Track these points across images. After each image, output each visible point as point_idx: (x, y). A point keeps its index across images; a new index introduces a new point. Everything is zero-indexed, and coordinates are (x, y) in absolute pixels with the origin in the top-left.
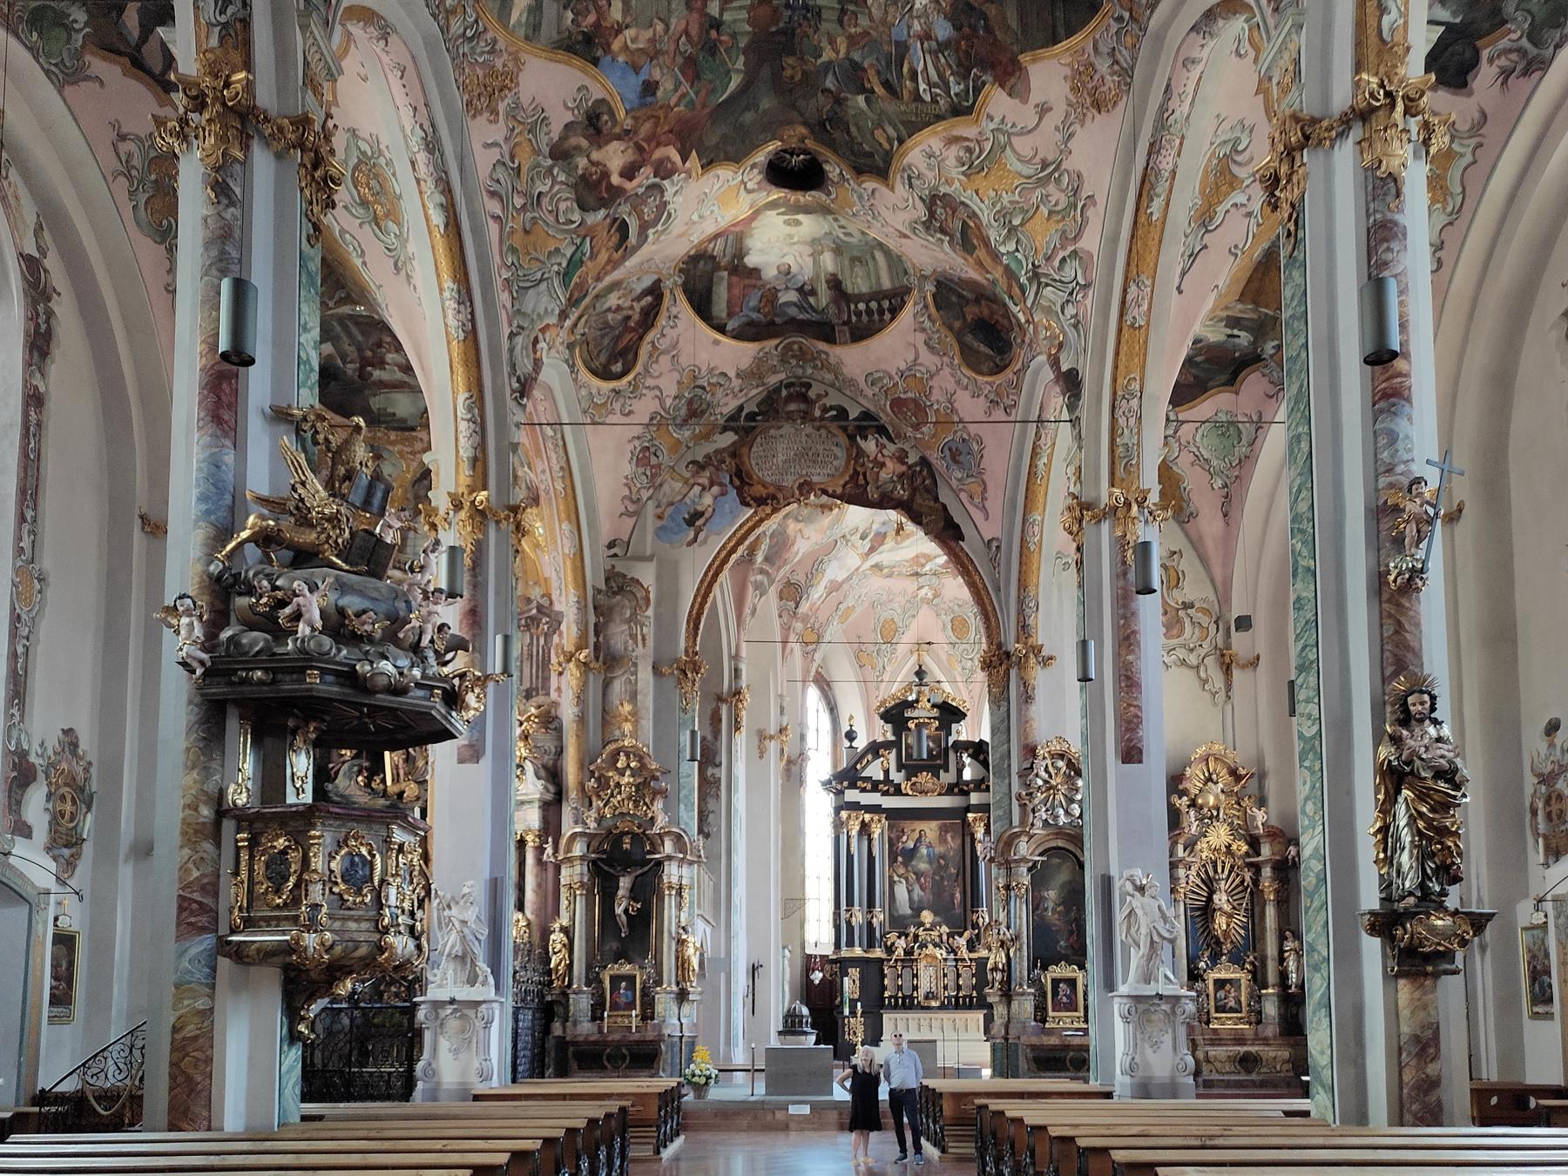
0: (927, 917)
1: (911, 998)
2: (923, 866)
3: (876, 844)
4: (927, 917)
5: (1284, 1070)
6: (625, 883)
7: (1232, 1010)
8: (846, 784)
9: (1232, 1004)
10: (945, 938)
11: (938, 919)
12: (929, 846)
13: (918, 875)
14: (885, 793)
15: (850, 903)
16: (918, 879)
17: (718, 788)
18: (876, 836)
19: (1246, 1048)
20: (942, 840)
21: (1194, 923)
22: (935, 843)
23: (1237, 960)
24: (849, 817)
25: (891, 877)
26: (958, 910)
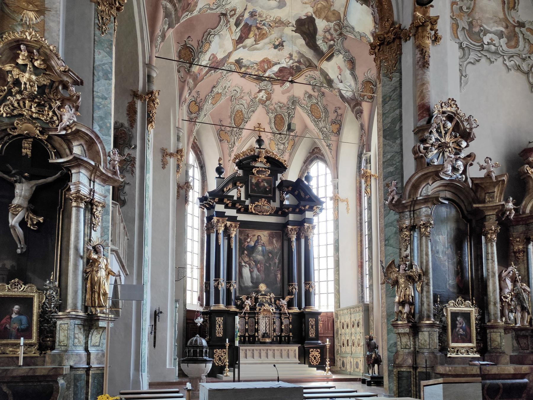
0: (263, 287)
1: (254, 337)
2: (259, 257)
3: (233, 240)
4: (263, 287)
6: (22, 191)
8: (217, 199)
10: (273, 300)
11: (268, 290)
12: (263, 245)
13: (256, 262)
14: (239, 211)
15: (217, 275)
16: (256, 265)
18: (233, 236)
20: (271, 242)
22: (266, 243)
24: (218, 221)
25: (240, 263)
26: (279, 285)
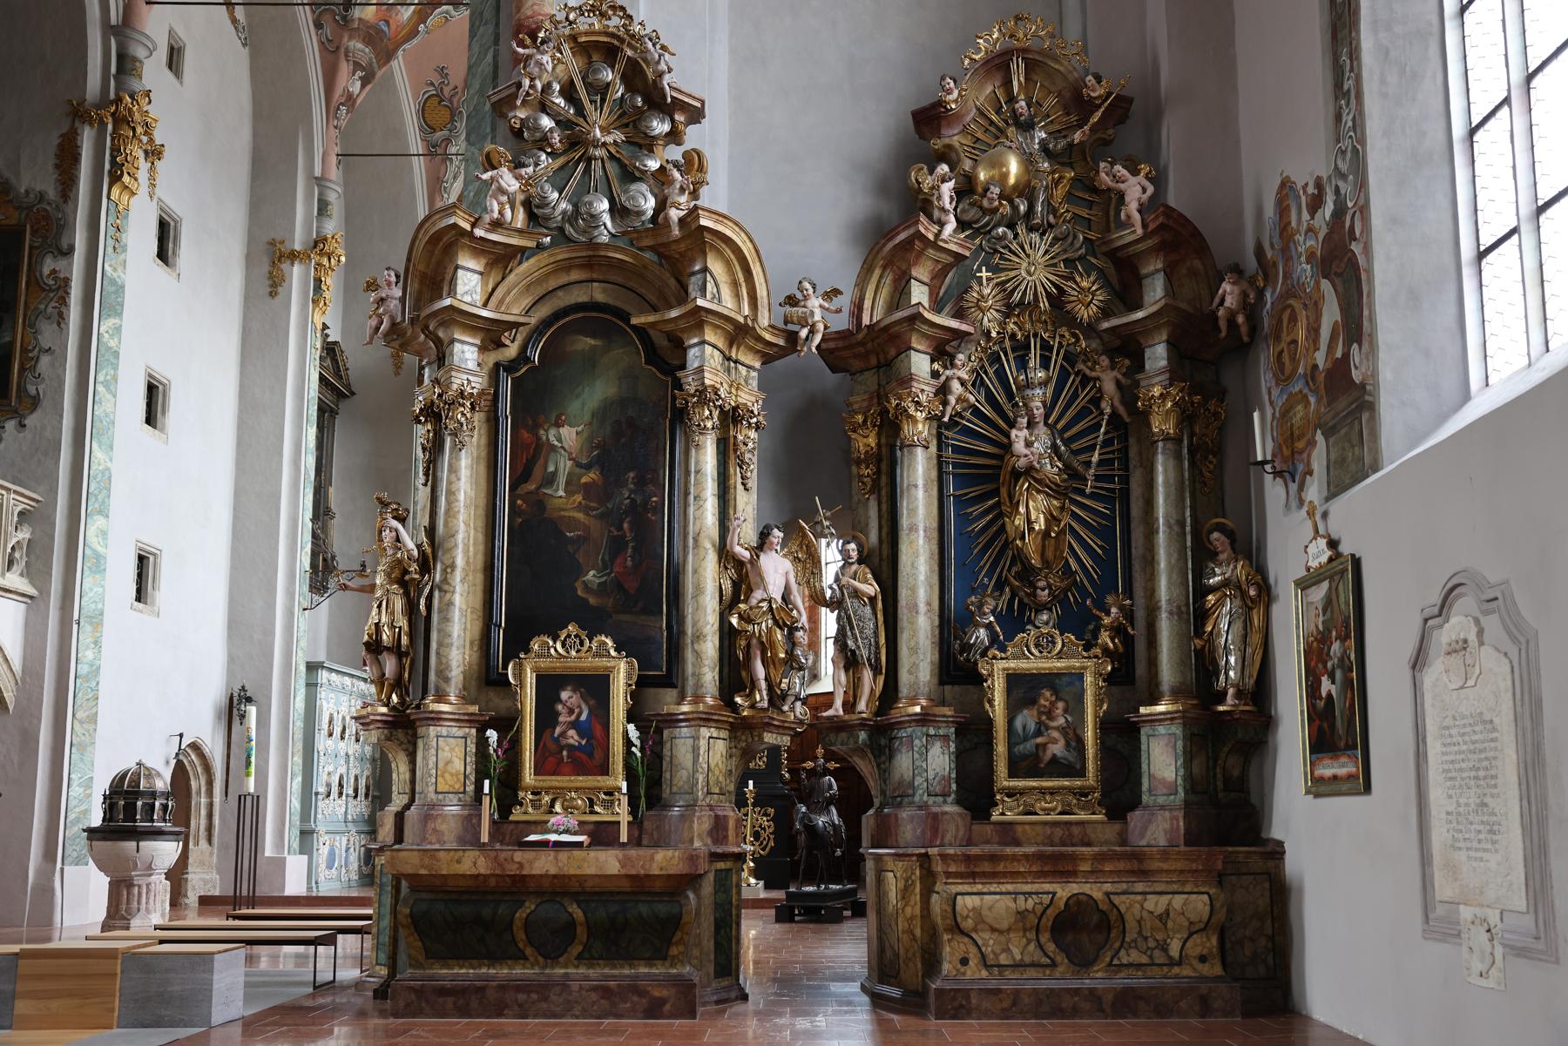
5: (1193, 959)
7: (1058, 768)
9: (1057, 749)
17: (63, 301)
19: (1074, 888)
21: (963, 519)
23: (1079, 623)
